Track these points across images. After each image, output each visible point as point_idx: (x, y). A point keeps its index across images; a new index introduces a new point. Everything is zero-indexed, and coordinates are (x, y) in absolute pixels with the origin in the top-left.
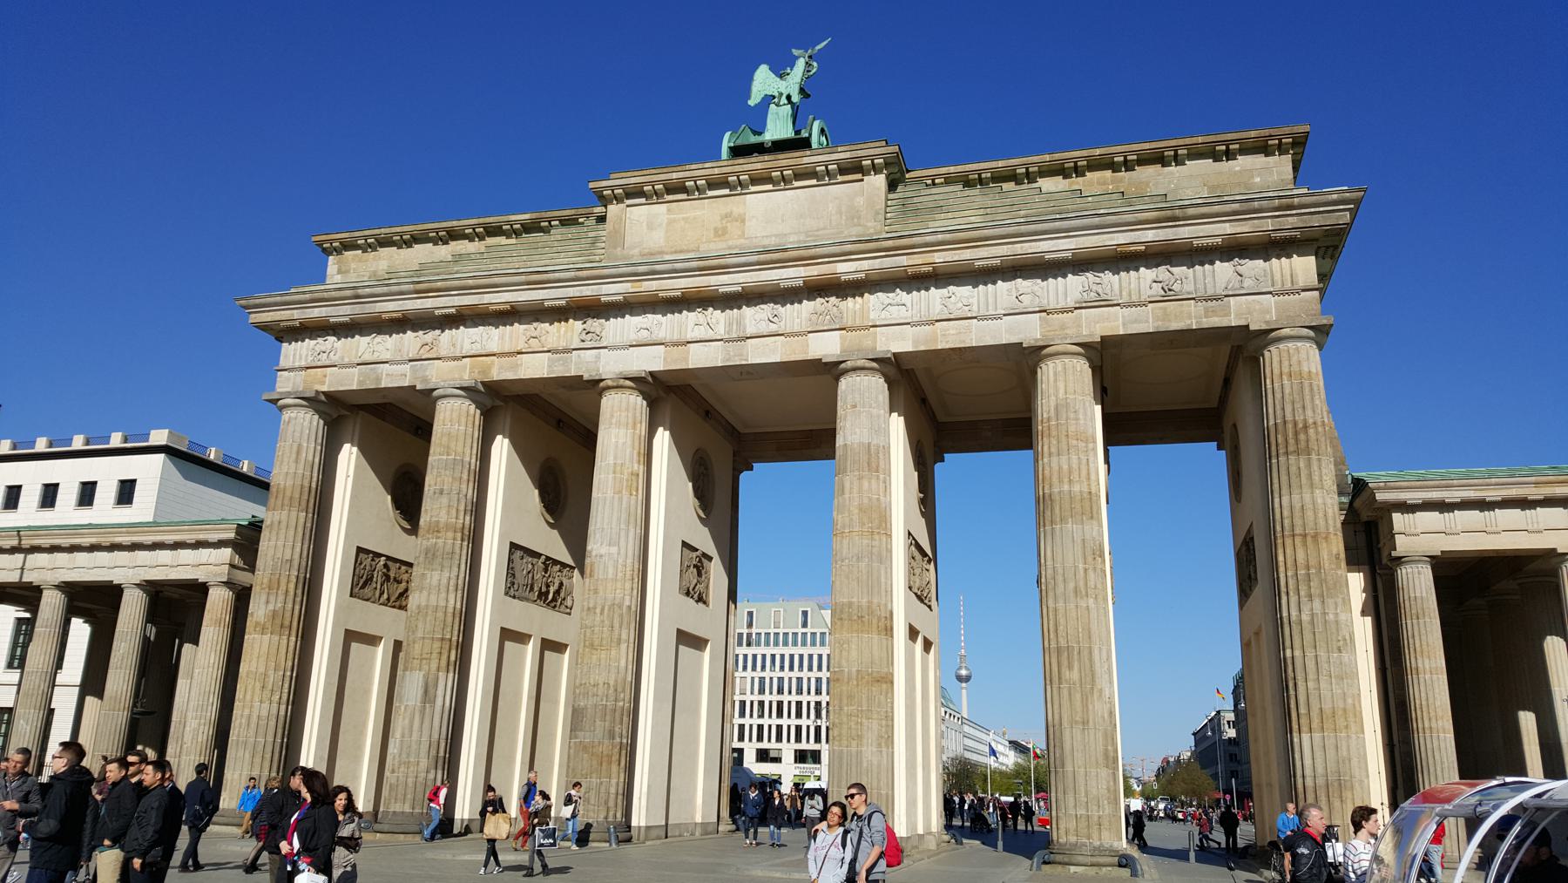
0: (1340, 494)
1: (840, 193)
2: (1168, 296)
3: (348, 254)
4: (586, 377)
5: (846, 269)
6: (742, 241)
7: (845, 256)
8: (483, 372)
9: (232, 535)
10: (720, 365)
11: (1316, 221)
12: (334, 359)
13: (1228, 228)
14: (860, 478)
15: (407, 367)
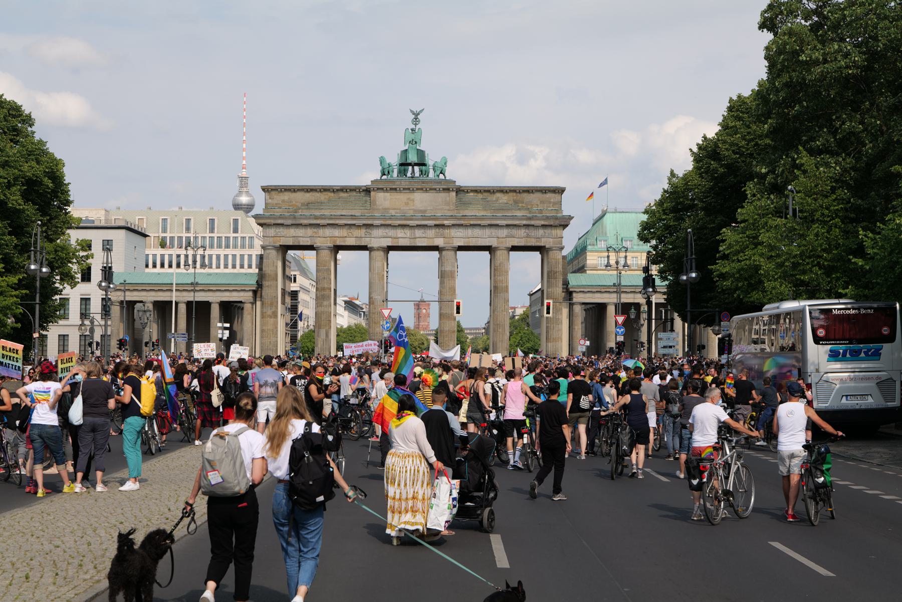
0: (563, 285)
1: (443, 195)
2: (528, 236)
3: (273, 193)
4: (369, 246)
5: (446, 222)
6: (413, 208)
7: (447, 219)
8: (335, 241)
9: (254, 289)
10: (408, 245)
11: (563, 223)
12: (283, 234)
13: (543, 223)
14: (449, 280)
15: (308, 239)
